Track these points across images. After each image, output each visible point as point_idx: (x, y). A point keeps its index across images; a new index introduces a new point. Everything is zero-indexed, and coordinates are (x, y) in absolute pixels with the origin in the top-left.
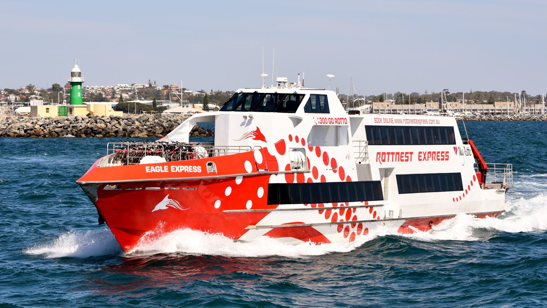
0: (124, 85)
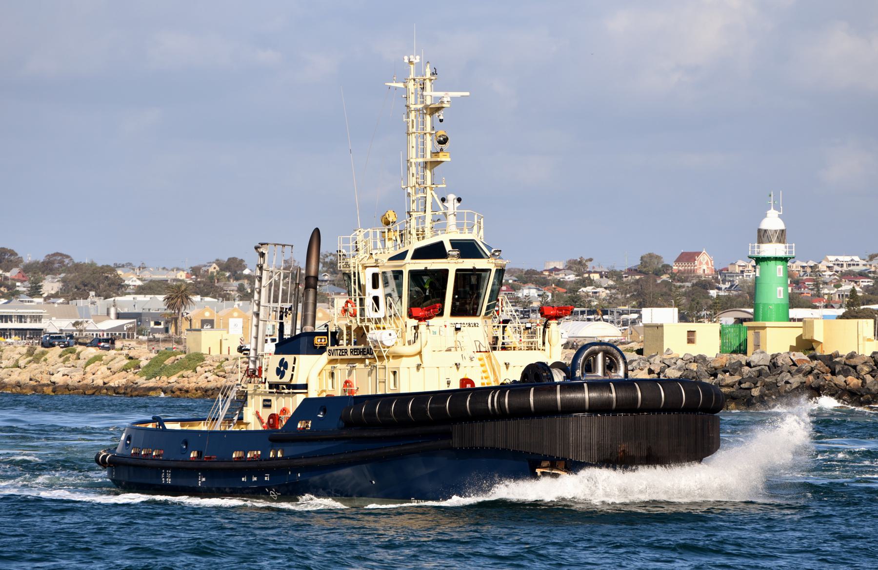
0: (848, 258)
